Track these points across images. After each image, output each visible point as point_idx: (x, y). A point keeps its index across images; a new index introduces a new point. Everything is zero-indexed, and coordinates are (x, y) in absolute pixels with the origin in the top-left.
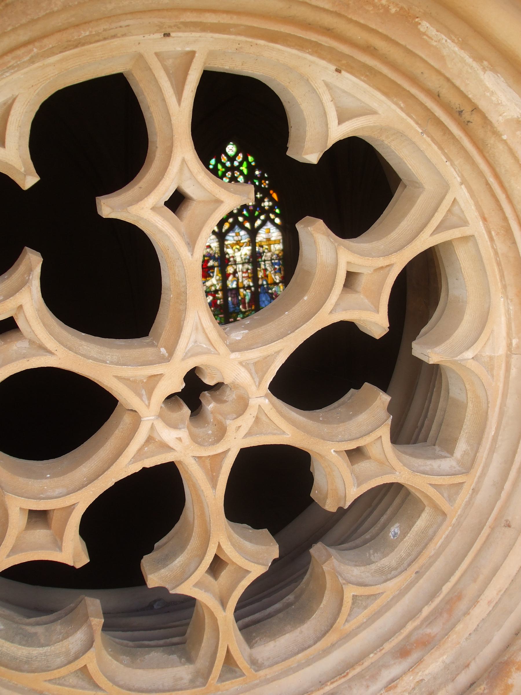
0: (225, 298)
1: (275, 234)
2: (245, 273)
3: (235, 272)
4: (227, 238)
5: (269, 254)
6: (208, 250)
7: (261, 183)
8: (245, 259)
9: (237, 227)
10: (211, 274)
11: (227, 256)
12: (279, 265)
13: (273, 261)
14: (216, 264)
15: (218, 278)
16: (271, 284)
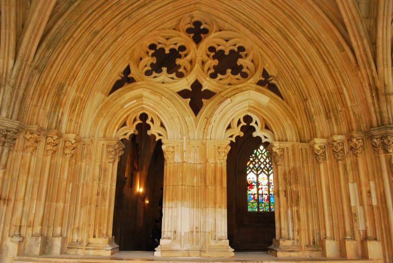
0: (258, 197)
3: (262, 188)
14: (255, 184)
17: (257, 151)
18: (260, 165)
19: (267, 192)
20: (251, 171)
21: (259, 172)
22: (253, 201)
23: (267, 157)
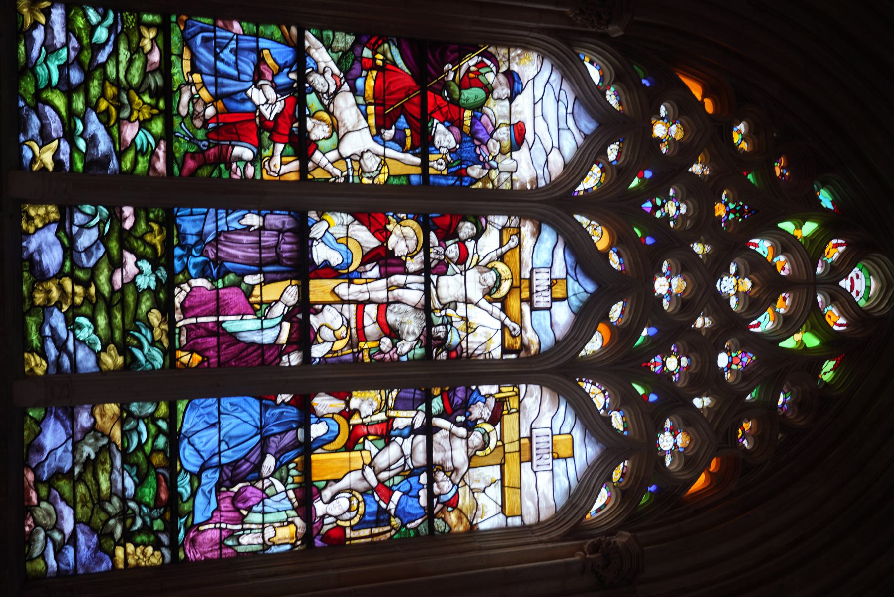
2: (381, 319)
3: (385, 260)
4: (548, 236)
5: (460, 457)
6: (503, 133)
7: (747, 411)
8: (448, 323)
9: (590, 288)
10: (389, 134)
11: (467, 229)
13: (423, 478)
14: (437, 164)
15: (371, 163)
16: (306, 469)
17: (832, 225)
18: (670, 243)
20: (607, 125)
21: (600, 238)
22: (194, 98)
23: (766, 345)
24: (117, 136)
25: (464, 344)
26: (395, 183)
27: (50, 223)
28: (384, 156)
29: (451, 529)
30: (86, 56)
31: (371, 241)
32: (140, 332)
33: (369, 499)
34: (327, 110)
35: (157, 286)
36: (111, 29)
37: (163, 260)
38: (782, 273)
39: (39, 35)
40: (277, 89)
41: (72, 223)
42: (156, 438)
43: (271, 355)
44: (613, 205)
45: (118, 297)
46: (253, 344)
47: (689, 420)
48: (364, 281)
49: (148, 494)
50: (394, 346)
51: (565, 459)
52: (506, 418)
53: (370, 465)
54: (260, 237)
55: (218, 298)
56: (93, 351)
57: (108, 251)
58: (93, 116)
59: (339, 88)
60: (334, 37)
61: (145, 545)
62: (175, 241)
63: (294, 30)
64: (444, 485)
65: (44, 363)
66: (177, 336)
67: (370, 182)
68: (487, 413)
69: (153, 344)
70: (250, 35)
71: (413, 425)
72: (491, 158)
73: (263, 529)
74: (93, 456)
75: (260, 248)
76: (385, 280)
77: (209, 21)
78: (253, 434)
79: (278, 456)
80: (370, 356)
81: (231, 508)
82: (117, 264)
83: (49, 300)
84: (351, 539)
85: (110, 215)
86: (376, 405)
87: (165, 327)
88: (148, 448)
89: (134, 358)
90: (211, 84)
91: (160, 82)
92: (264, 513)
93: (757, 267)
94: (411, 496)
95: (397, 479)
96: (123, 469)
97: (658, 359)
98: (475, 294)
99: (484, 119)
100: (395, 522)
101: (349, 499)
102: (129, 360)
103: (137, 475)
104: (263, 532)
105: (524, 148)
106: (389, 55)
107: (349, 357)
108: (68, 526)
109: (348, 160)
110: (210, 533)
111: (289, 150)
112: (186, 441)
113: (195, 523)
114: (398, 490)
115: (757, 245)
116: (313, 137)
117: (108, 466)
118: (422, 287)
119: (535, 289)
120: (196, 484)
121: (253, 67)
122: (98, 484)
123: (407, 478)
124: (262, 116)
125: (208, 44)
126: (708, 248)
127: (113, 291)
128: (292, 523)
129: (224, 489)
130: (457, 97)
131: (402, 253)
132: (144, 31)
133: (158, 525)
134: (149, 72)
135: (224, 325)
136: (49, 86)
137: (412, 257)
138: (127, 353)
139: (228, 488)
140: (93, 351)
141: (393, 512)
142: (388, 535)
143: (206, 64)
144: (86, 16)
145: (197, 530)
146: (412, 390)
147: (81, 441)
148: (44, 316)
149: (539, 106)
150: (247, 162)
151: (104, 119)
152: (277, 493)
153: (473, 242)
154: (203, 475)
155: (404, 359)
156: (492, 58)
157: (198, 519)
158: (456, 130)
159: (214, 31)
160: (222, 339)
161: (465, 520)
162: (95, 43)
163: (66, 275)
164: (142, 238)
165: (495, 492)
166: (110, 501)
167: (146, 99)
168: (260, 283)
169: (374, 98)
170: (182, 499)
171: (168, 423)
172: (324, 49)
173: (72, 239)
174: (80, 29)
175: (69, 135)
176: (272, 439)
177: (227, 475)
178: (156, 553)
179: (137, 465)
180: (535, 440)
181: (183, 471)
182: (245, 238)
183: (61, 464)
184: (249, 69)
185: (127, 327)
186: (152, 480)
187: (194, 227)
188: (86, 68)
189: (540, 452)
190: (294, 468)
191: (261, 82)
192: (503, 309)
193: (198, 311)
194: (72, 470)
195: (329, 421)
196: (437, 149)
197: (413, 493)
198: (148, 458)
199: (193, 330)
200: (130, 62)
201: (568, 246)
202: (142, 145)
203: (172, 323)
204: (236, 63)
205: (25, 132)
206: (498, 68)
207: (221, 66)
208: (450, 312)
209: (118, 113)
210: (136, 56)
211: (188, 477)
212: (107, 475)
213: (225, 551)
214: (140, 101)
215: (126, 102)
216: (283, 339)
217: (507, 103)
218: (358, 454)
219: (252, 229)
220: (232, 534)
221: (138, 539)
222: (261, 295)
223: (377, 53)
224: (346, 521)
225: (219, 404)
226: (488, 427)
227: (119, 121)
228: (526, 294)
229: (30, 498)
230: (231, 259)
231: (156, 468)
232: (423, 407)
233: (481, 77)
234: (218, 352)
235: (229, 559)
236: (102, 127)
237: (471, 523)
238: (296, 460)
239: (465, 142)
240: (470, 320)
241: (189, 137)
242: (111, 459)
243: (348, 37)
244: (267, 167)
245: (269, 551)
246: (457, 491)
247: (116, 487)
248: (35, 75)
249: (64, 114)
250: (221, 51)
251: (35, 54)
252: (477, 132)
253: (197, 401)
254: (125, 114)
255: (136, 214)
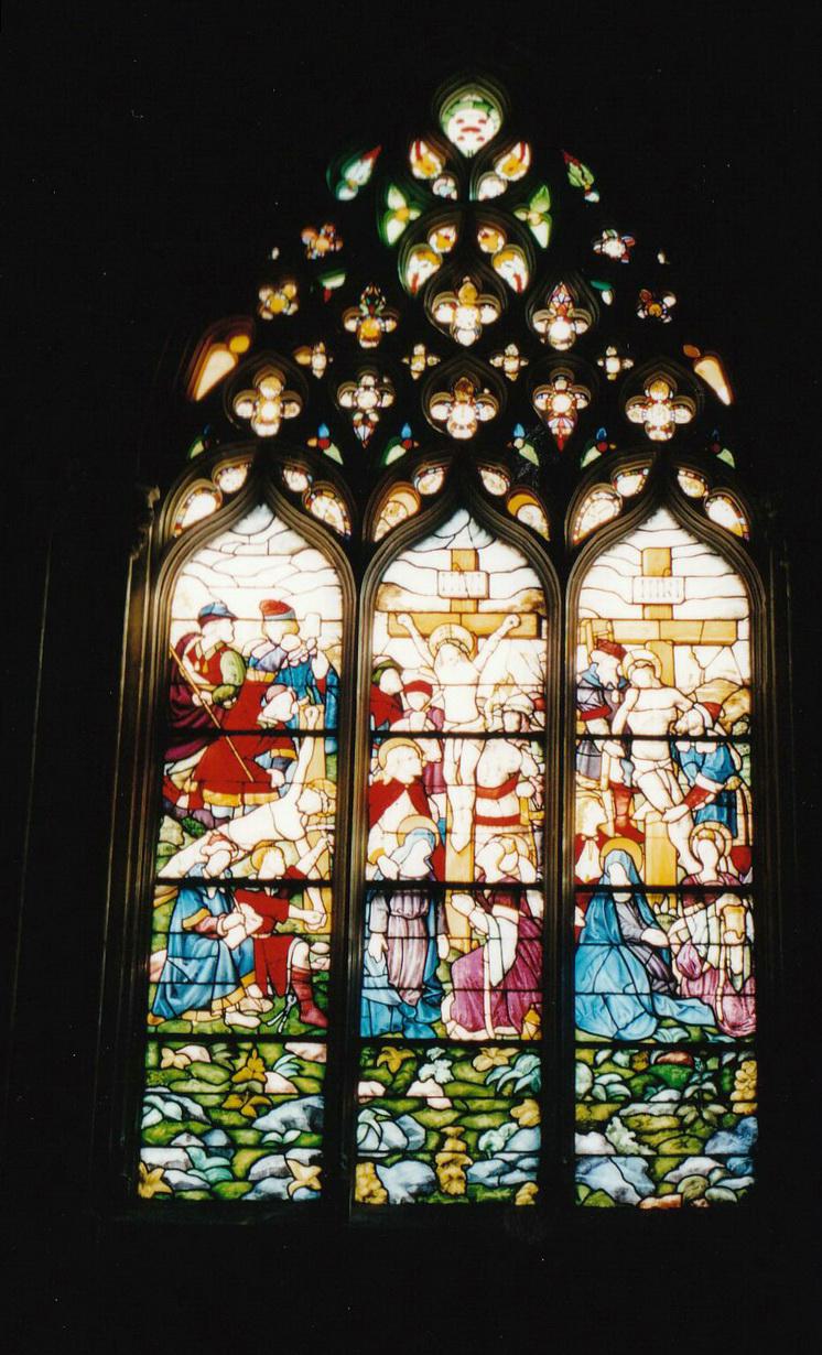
1: (712, 591)
3: (423, 789)
4: (394, 573)
6: (276, 628)
10: (277, 778)
12: (722, 778)
13: (682, 746)
14: (313, 718)
16: (663, 891)
18: (409, 403)
19: (507, 857)
24: (283, 1097)
25: (528, 689)
26: (335, 772)
27: (376, 1173)
28: (303, 784)
29: (746, 714)
30: (197, 1127)
31: (403, 804)
32: (498, 1080)
33: (703, 817)
34: (250, 853)
35: (448, 1059)
36: (166, 1100)
37: (420, 1052)
38: (453, 239)
39: (175, 1177)
40: (228, 911)
41: (377, 1151)
42: (616, 1064)
43: (531, 929)
44: (362, 483)
45: (458, 1103)
46: (517, 951)
47: (634, 386)
48: (449, 814)
49: (677, 1074)
50: (527, 779)
51: (671, 559)
52: (619, 636)
53: (663, 814)
54: (394, 938)
55: (465, 990)
56: (517, 1132)
57: (408, 1113)
58: (261, 1123)
59: (224, 838)
60: (166, 842)
61: (734, 1079)
62: (399, 1036)
63: (160, 889)
64: (693, 721)
65: (527, 1185)
66: (505, 1038)
67: (333, 803)
68: (612, 661)
69: (513, 1067)
70: (168, 942)
71: (620, 758)
72: (303, 647)
73: (726, 945)
74: (633, 1134)
75: (408, 938)
76: (449, 788)
77: (152, 990)
78: (618, 954)
79: (644, 926)
80: (538, 810)
81: (700, 982)
82: (423, 1103)
83: (460, 1178)
84: (747, 840)
85: (369, 1108)
86: (593, 804)
87: (493, 1051)
88: (628, 1074)
89: (527, 1087)
90: (224, 990)
91: (222, 1046)
92: (708, 944)
93: (444, 282)
94: (703, 763)
95: (682, 779)
96: (648, 1102)
97: (553, 424)
98: (467, 671)
99: (258, 654)
100: (732, 783)
101: (700, 839)
102: (527, 1094)
103: (656, 1086)
104: (730, 946)
105: (289, 602)
106: (187, 774)
107: (538, 836)
108: (705, 1164)
109: (308, 829)
110: (728, 1008)
111: (297, 899)
112: (622, 1032)
113: (713, 1023)
114: (694, 778)
115: (416, 277)
116: (281, 871)
117: (644, 1119)
118: (459, 741)
119: (465, 595)
120: (671, 1022)
121: (204, 940)
122: (663, 1130)
123: (681, 767)
124: (258, 931)
125: (179, 991)
126: (419, 349)
127: (453, 1108)
128: (722, 911)
129: (678, 991)
130: (232, 690)
131: (419, 765)
132: (164, 1064)
133: (712, 1064)
134: (211, 1058)
135: (494, 984)
136: (229, 1168)
137: (423, 752)
138: (522, 1095)
139: (677, 985)
140: (517, 1132)
141: (720, 787)
142: (747, 793)
143: (202, 995)
144: (153, 1126)
145: (722, 1022)
146: (578, 756)
147: (615, 1147)
148: (477, 1184)
149: (242, 582)
150: (310, 950)
151: (264, 1110)
152: (687, 927)
153: (404, 673)
154: (661, 1013)
155: (542, 767)
156: (183, 642)
157: (710, 1020)
158: (271, 692)
159: (165, 984)
160: (510, 986)
161: (736, 695)
162: (182, 1117)
163: (434, 1159)
164: (394, 1075)
165: (705, 653)
166: (684, 1117)
167: (240, 1063)
168: (448, 939)
169: (234, 793)
170: (686, 1038)
171: (600, 1050)
172: (181, 853)
173: (393, 1151)
174: (167, 1133)
175: (282, 1148)
176: (624, 933)
177: (662, 986)
178: (744, 1066)
179: (645, 1086)
180: (647, 601)
181: (655, 1036)
182: (396, 956)
183: (640, 1169)
184: (205, 946)
185: (492, 1094)
186: (662, 1071)
187: (383, 1015)
188: (208, 1127)
189: (661, 594)
190: (660, 907)
191: (220, 932)
192: (486, 636)
193: (477, 1014)
194: (646, 1158)
195: (608, 860)
196: (294, 717)
197: (700, 761)
198: (638, 1074)
199: (499, 1019)
200: (200, 1079)
201: (409, 548)
202: (293, 1069)
203: (490, 1043)
204: (199, 959)
205: (280, 1194)
206: (194, 634)
207: (203, 978)
208: (487, 708)
209: (258, 1094)
210: (193, 1073)
211: (662, 1030)
212: (654, 1119)
213: (748, 991)
214: (244, 1070)
215: (245, 1085)
216: (514, 914)
217: (235, 623)
218: (648, 827)
219: (386, 947)
220: (730, 980)
221: (727, 1087)
222: (462, 939)
223: (183, 789)
224: (725, 844)
225: (581, 993)
226: (628, 660)
227: (264, 1094)
228: (470, 606)
229: (674, 1203)
230: (421, 973)
231: (650, 1065)
232: (599, 744)
233: (208, 657)
234: (525, 991)
235: (758, 986)
236: (273, 1112)
237: (741, 688)
238: (650, 902)
239: (284, 680)
240: (498, 680)
241: (283, 1016)
242: (636, 1115)
243: (165, 825)
244: (315, 927)
245: (752, 938)
246: (700, 703)
247: (668, 1110)
248: (218, 1182)
249: (259, 1153)
250: (186, 976)
251: (196, 1182)
252: (274, 666)
253: (578, 1020)
254: (258, 1087)
255: (369, 1079)
